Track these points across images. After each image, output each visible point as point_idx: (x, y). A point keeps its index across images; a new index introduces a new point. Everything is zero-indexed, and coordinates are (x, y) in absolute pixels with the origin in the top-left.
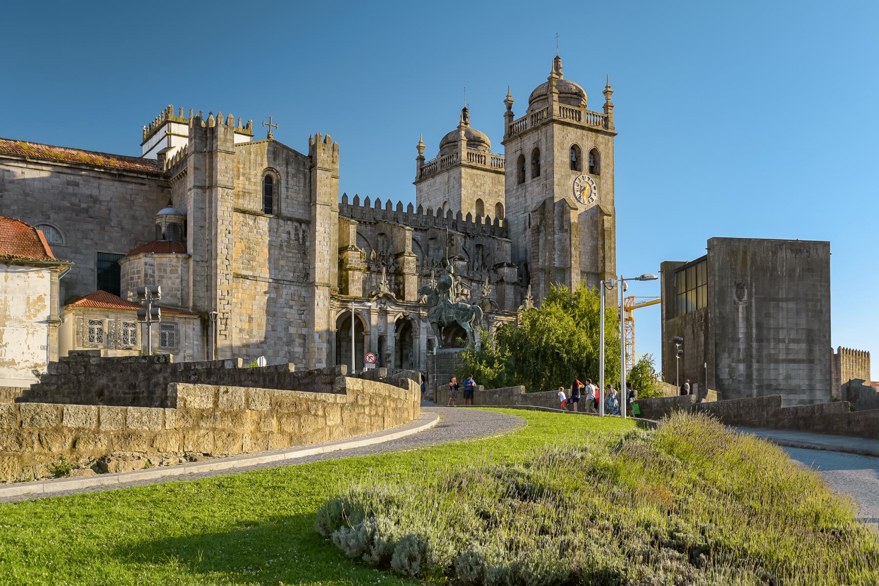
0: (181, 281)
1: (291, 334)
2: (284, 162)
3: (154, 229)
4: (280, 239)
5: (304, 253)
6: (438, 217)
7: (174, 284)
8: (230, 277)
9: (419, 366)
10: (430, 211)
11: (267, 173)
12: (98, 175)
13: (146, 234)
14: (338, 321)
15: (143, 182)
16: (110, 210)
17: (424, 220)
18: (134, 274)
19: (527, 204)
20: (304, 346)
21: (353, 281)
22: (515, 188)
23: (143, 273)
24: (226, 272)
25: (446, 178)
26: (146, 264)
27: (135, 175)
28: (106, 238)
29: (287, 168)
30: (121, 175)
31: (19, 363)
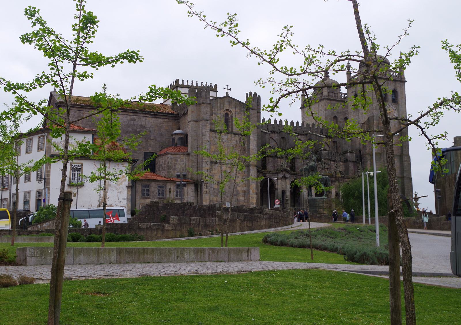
0: (185, 165)
1: (238, 190)
2: (234, 107)
3: (171, 140)
4: (232, 144)
5: (244, 150)
6: (312, 128)
7: (182, 167)
8: (209, 163)
9: (303, 205)
10: (308, 125)
11: (226, 112)
12: (145, 115)
13: (167, 142)
14: (261, 183)
15: (166, 118)
16: (150, 131)
17: (305, 129)
18: (163, 162)
19: (360, 120)
20: (245, 196)
21: (269, 162)
22: (353, 111)
23: (167, 162)
24: (207, 161)
25: (317, 105)
26: (168, 158)
27: (162, 114)
28: (148, 145)
29: (235, 109)
30: (155, 115)
31: (114, 206)
